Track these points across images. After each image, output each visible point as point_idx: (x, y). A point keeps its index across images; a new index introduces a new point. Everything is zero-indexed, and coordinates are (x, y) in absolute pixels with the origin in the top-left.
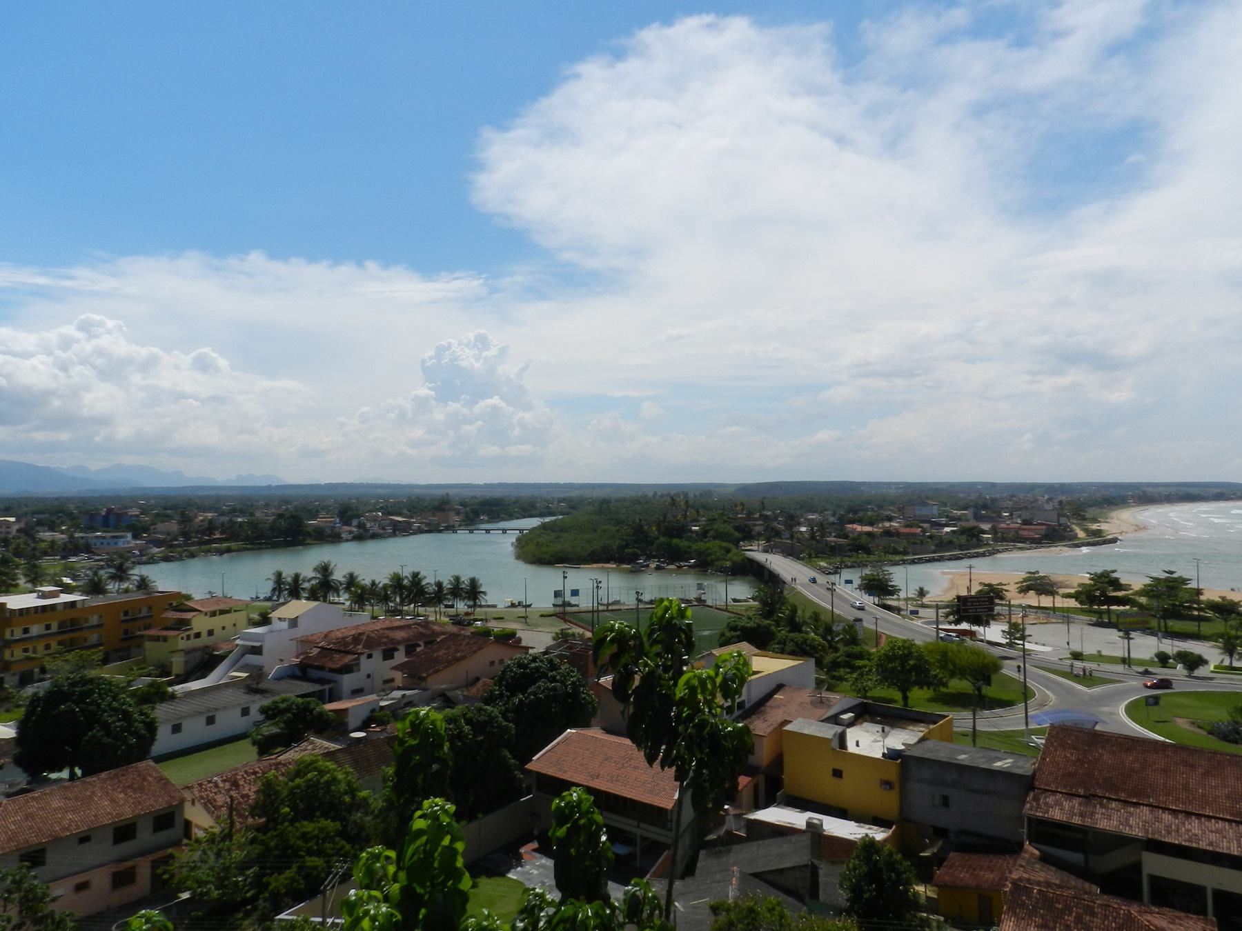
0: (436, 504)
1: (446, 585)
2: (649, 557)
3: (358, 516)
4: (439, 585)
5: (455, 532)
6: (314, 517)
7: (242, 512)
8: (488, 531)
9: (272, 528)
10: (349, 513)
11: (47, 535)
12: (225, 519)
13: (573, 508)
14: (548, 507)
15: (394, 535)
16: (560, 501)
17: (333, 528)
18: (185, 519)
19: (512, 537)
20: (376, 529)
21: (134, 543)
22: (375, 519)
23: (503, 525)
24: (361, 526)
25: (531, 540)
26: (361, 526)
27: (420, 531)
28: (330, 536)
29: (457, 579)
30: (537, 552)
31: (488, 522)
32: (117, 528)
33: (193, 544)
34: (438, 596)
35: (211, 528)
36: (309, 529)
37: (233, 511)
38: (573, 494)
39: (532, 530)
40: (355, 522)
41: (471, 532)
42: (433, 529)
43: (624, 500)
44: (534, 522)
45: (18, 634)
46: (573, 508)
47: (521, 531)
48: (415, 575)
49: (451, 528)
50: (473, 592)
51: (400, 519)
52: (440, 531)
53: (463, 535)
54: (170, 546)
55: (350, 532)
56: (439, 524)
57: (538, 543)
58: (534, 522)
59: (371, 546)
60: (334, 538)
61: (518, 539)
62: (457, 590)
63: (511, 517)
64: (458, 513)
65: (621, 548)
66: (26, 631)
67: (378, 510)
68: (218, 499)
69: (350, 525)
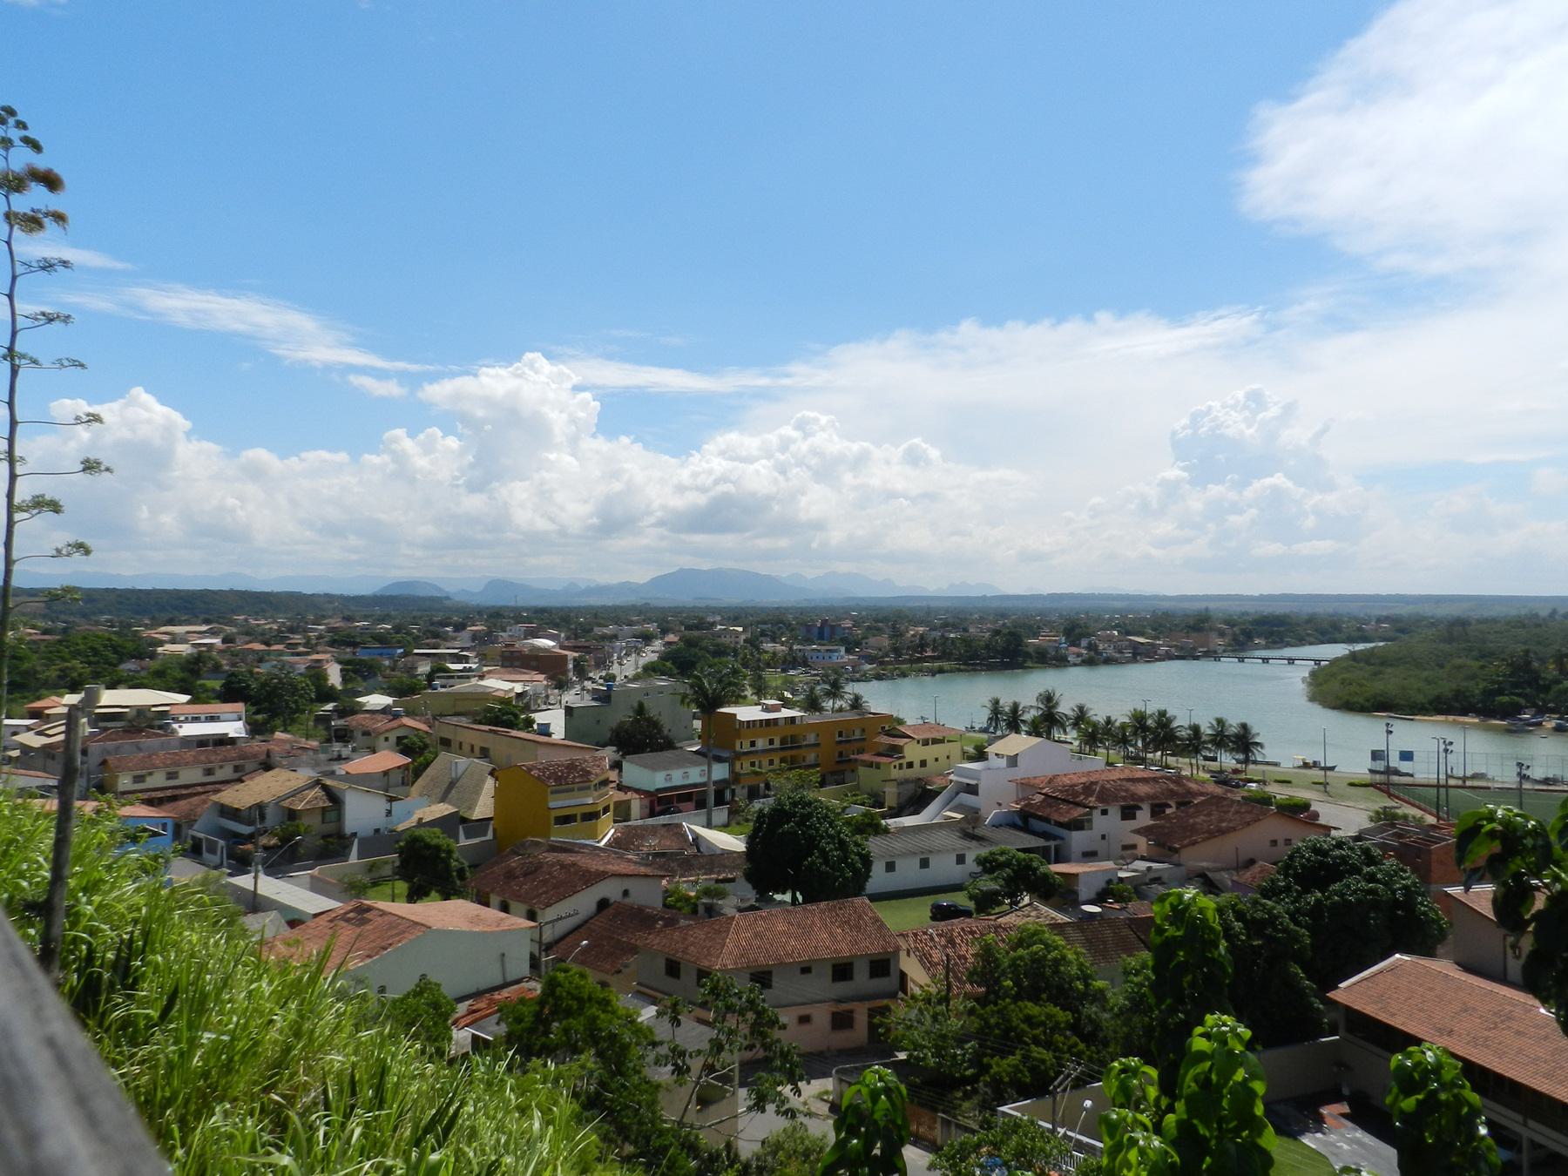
0: (1192, 623)
1: (1206, 730)
2: (1542, 711)
4: (1196, 729)
5: (1217, 659)
7: (955, 627)
9: (987, 647)
11: (768, 646)
13: (1402, 631)
14: (1360, 629)
15: (1134, 659)
16: (1379, 620)
17: (1057, 649)
18: (897, 634)
19: (1303, 671)
20: (1111, 652)
21: (847, 658)
22: (1110, 639)
24: (1091, 647)
25: (1334, 675)
27: (1169, 657)
28: (1055, 658)
29: (1220, 722)
31: (1267, 647)
32: (831, 642)
33: (903, 662)
35: (922, 644)
37: (945, 625)
38: (1404, 611)
39: (1334, 662)
41: (1241, 660)
42: (1188, 655)
43: (1495, 621)
44: (1339, 650)
45: (747, 748)
46: (1402, 631)
47: (1317, 662)
48: (1162, 714)
49: (1212, 655)
50: (1243, 742)
52: (1197, 658)
53: (1228, 664)
54: (882, 663)
55: (1079, 655)
56: (1194, 649)
57: (1343, 682)
58: (1339, 650)
59: (1104, 673)
60: (1061, 662)
61: (1313, 674)
62: (1221, 738)
63: (1301, 641)
64: (1222, 634)
65: (1489, 694)
66: (753, 744)
68: (929, 611)
69: (1078, 646)
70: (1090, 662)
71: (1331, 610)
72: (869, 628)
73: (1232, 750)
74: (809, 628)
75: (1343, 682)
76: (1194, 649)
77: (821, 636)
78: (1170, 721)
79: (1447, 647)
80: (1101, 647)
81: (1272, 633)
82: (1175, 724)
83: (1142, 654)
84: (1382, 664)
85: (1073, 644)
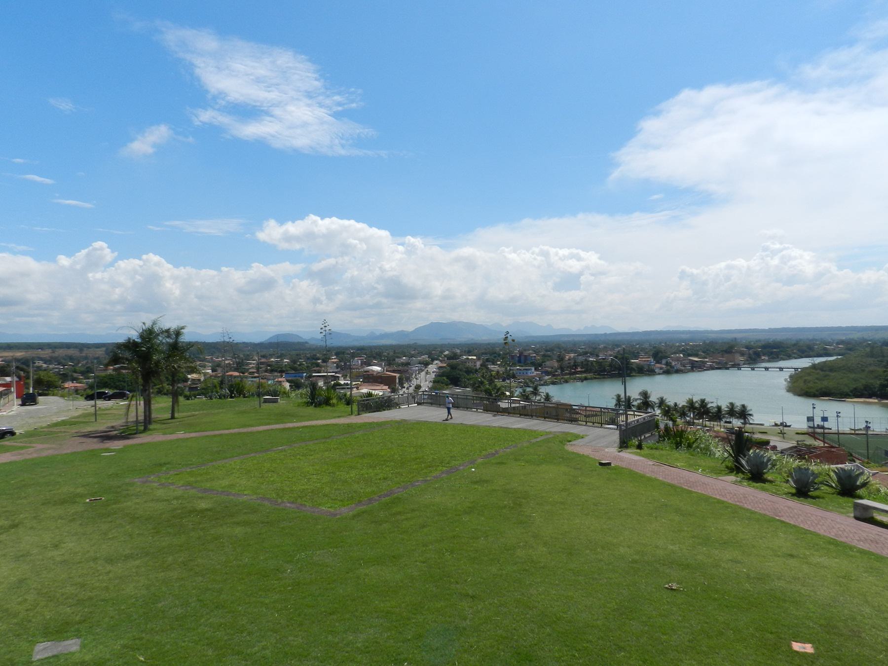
1: (724, 408)
3: (666, 357)
4: (719, 408)
5: (739, 369)
6: (636, 357)
7: (592, 354)
8: (767, 369)
9: (610, 365)
10: (660, 355)
11: (491, 367)
12: (581, 359)
13: (850, 350)
14: (825, 349)
16: (838, 343)
18: (561, 359)
19: (786, 374)
20: (679, 366)
22: (678, 359)
23: (782, 364)
26: (667, 364)
27: (712, 368)
30: (806, 387)
31: (769, 361)
32: (526, 365)
34: (717, 415)
35: (575, 366)
36: (634, 366)
40: (664, 361)
41: (753, 369)
46: (850, 350)
47: (796, 369)
48: (703, 401)
49: (737, 366)
50: (743, 414)
51: (696, 359)
52: (727, 369)
55: (661, 368)
56: (726, 363)
59: (675, 378)
60: (651, 372)
61: (791, 377)
62: (732, 412)
63: (789, 357)
64: (742, 354)
67: (681, 352)
70: (667, 372)
71: (811, 337)
72: (544, 356)
73: (737, 418)
74: (513, 357)
75: (805, 381)
76: (726, 363)
77: (519, 361)
78: (706, 404)
79: (870, 360)
80: (673, 364)
81: (772, 353)
82: (709, 406)
83: (696, 367)
84: (831, 370)
85: (658, 362)
